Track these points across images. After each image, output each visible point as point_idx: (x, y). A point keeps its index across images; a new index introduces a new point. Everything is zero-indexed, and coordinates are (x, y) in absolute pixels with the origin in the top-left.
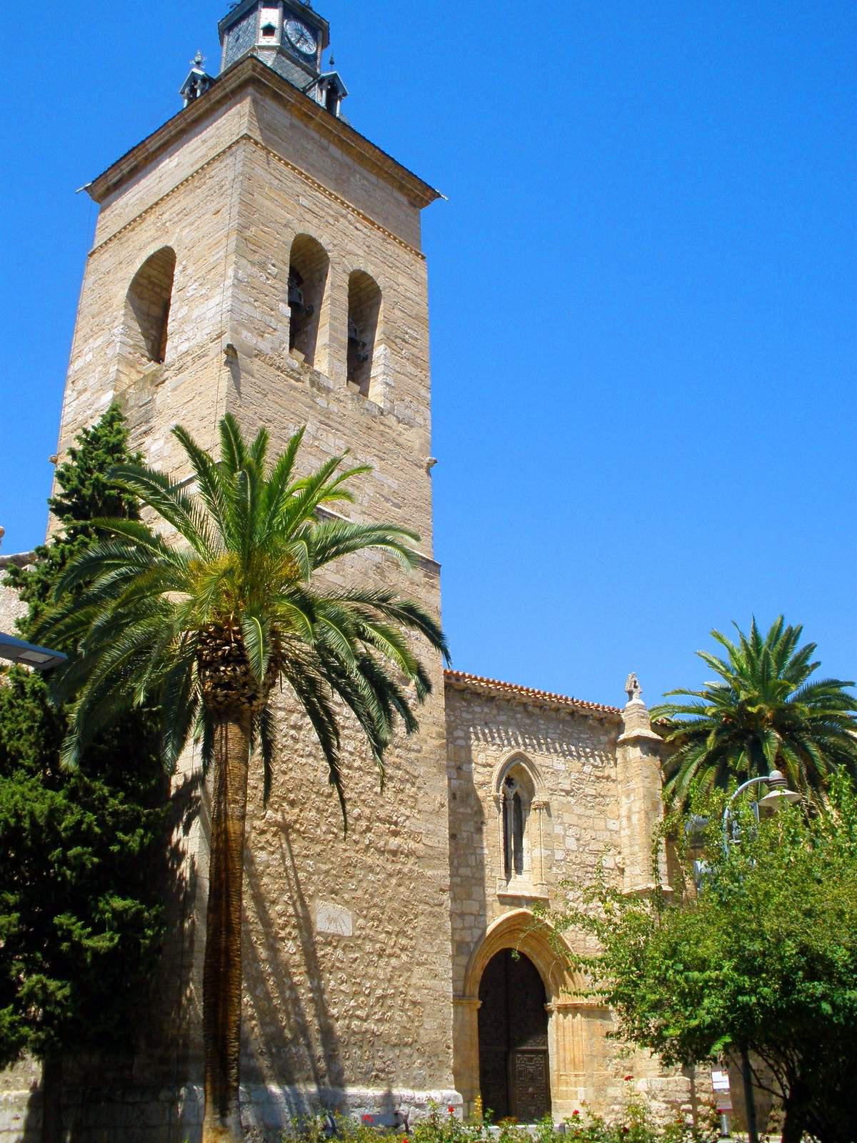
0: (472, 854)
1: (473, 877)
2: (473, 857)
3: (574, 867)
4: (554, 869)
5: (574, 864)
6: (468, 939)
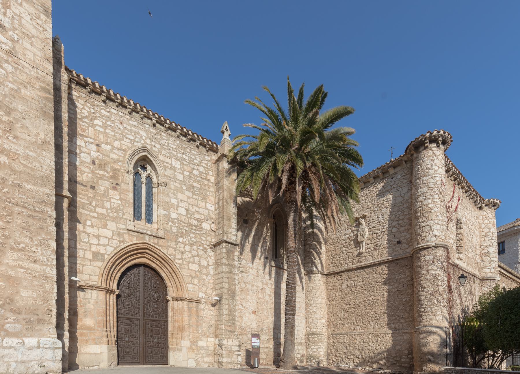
0: (107, 201)
1: (108, 215)
2: (108, 203)
3: (184, 224)
4: (170, 223)
5: (184, 222)
6: (102, 251)
